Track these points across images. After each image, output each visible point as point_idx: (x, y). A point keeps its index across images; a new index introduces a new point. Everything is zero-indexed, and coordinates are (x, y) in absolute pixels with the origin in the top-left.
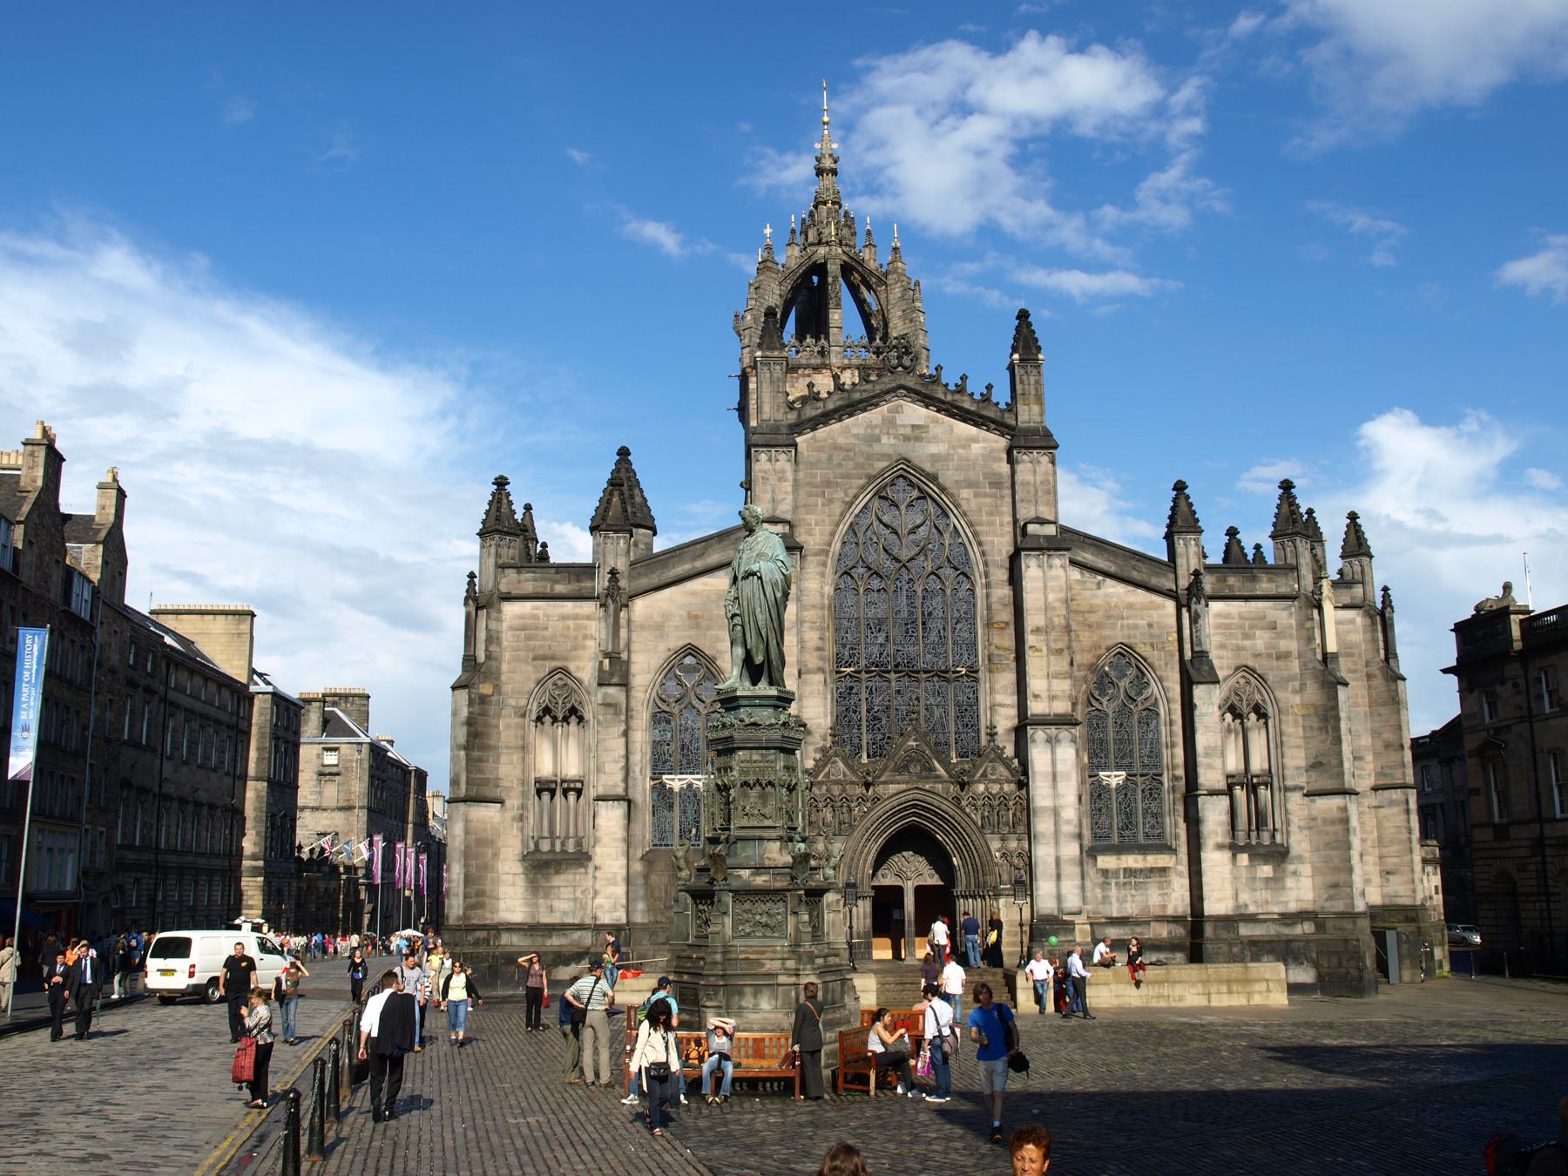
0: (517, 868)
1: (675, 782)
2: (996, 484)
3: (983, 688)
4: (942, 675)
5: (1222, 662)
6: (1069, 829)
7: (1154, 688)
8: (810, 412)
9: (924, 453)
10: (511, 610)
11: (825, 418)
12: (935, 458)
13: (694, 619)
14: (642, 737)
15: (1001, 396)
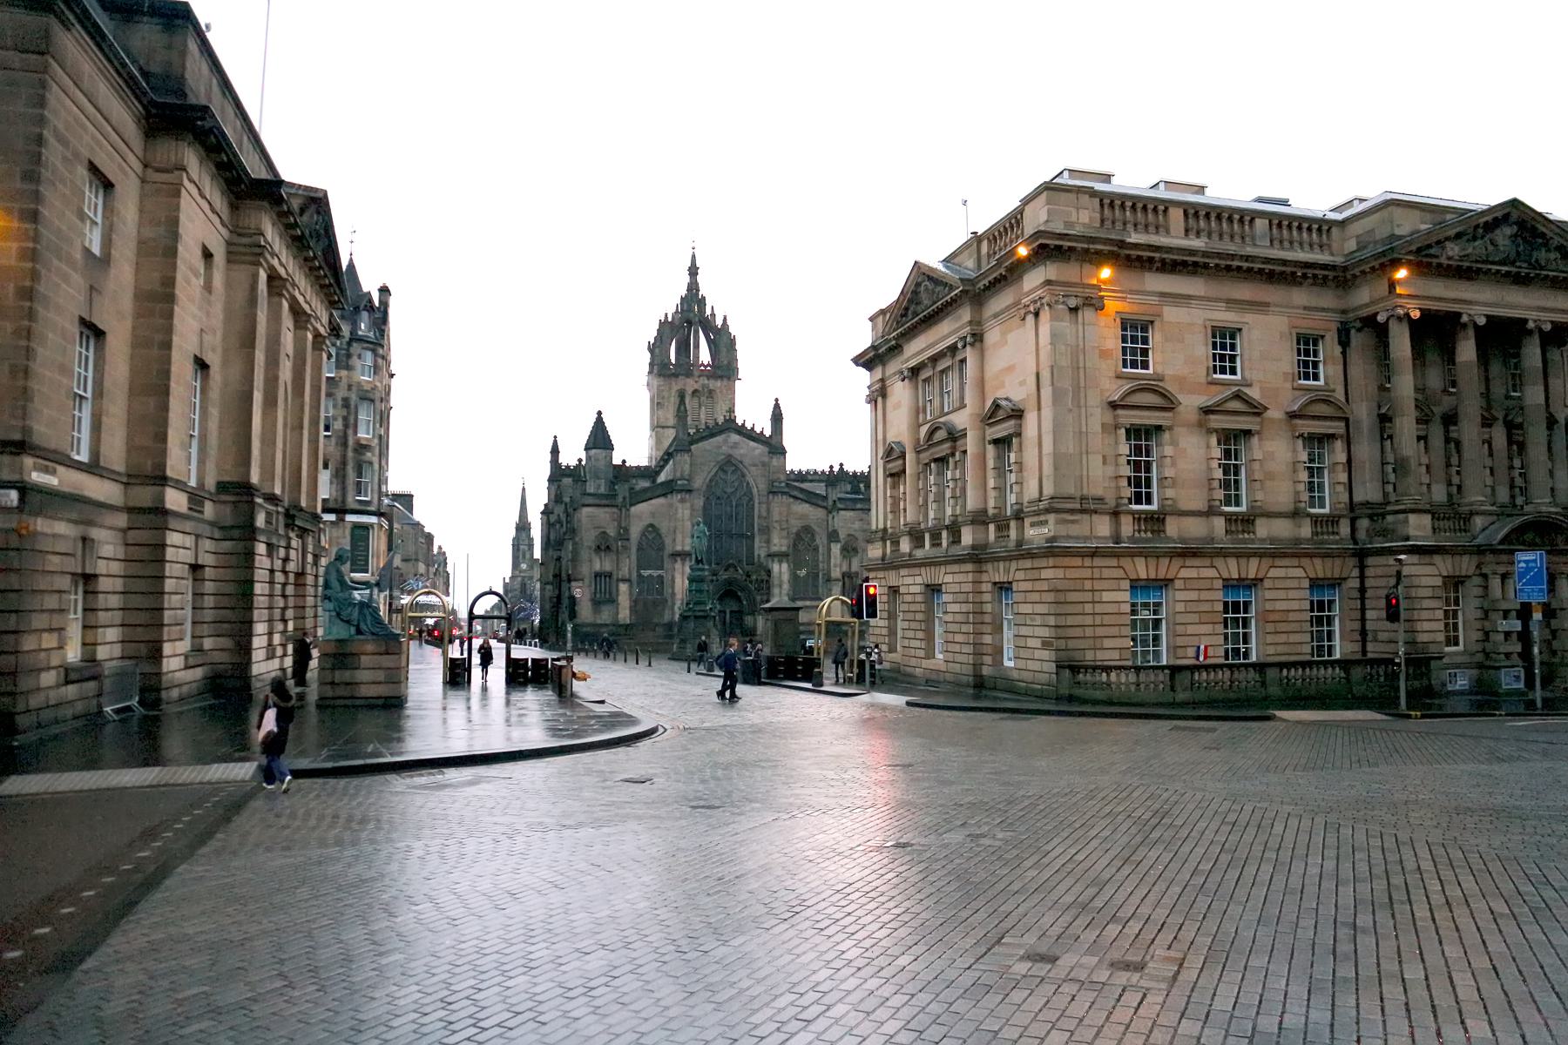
0: (589, 604)
1: (646, 573)
2: (764, 464)
3: (757, 540)
4: (742, 536)
5: (842, 536)
6: (784, 592)
7: (818, 541)
8: (696, 437)
9: (737, 453)
10: (586, 510)
11: (703, 439)
12: (741, 455)
13: (653, 514)
14: (634, 557)
15: (768, 433)
